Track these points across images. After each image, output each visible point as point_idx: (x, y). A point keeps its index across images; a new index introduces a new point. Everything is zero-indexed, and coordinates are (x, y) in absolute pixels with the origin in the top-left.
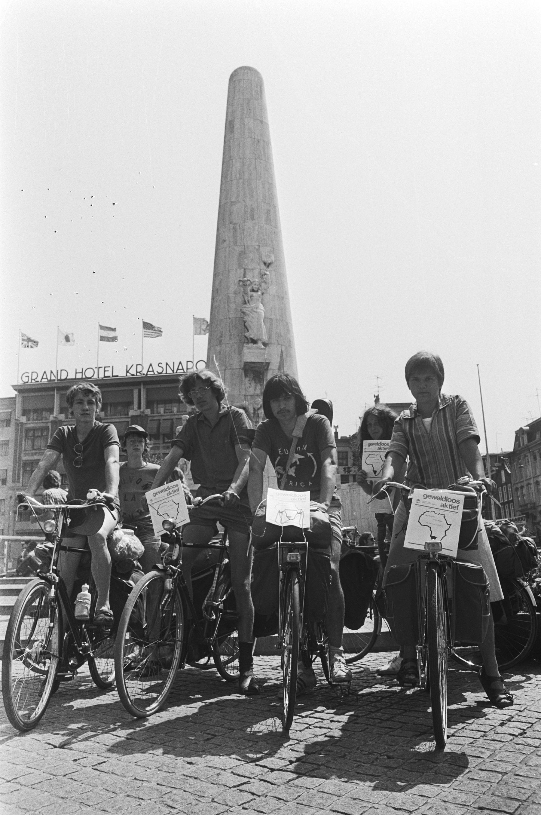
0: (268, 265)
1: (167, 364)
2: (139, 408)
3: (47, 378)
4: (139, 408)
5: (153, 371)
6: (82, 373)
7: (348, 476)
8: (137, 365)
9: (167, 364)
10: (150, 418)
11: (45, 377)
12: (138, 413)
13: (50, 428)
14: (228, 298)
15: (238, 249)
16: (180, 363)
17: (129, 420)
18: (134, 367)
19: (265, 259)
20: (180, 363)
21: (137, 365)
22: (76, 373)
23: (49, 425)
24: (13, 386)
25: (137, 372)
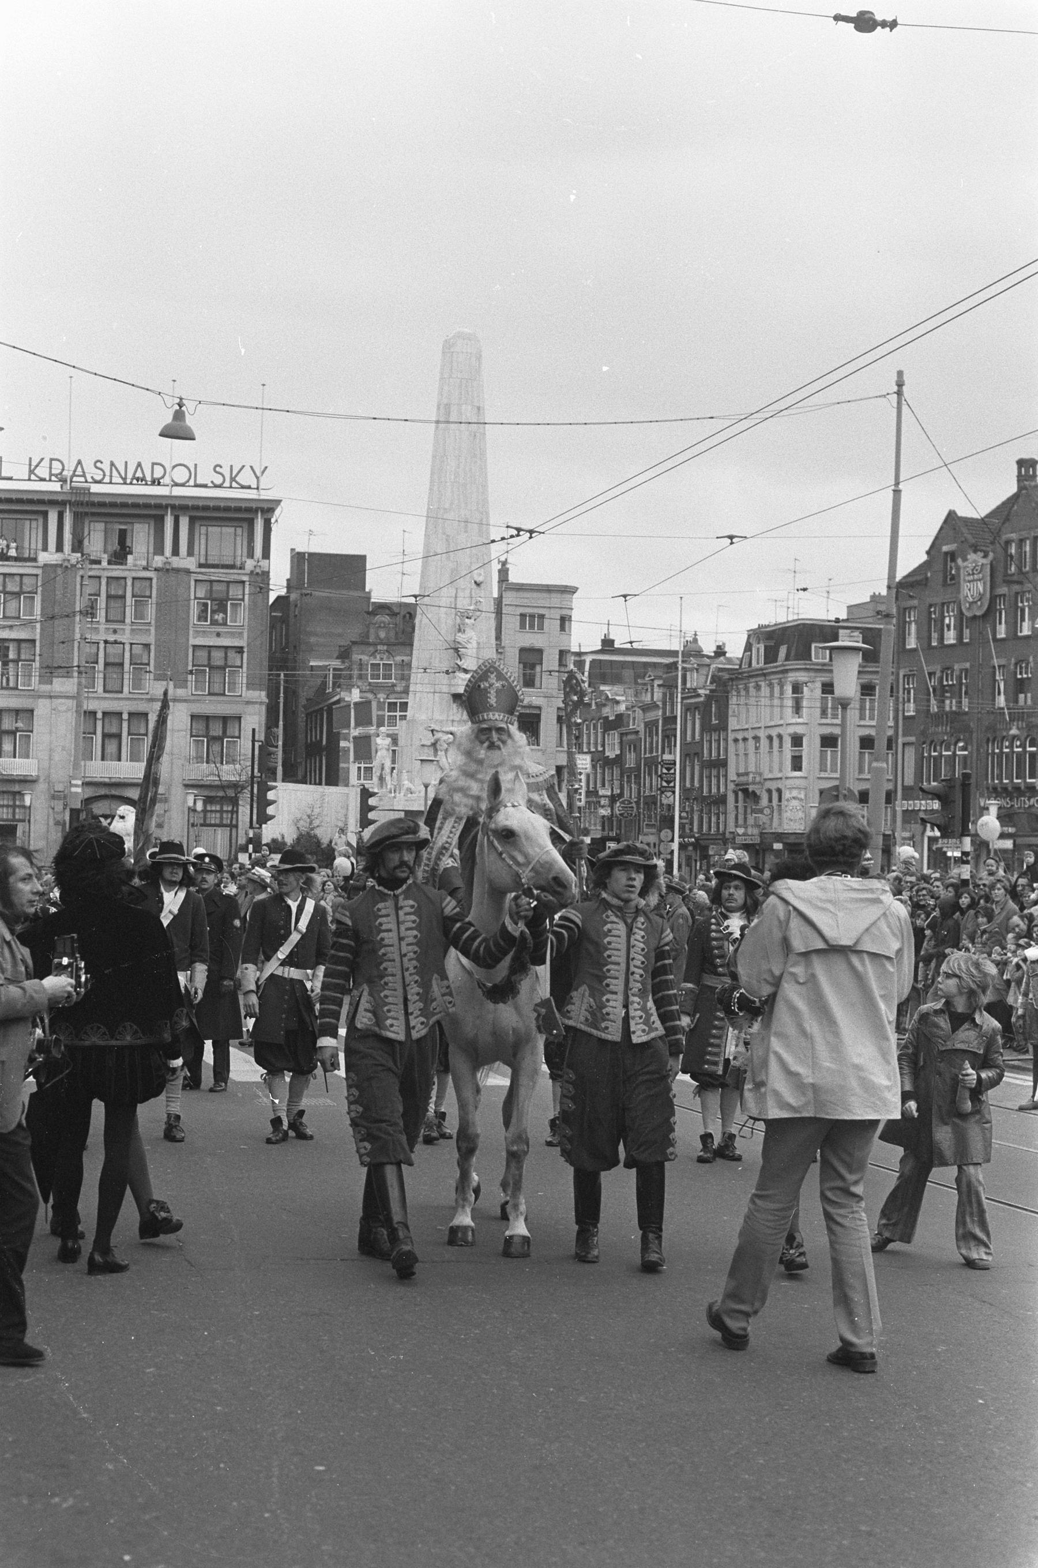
1: (112, 464)
2: (60, 548)
5: (84, 476)
8: (51, 460)
9: (112, 464)
16: (139, 465)
18: (46, 463)
20: (139, 465)
21: (51, 460)
25: (51, 475)
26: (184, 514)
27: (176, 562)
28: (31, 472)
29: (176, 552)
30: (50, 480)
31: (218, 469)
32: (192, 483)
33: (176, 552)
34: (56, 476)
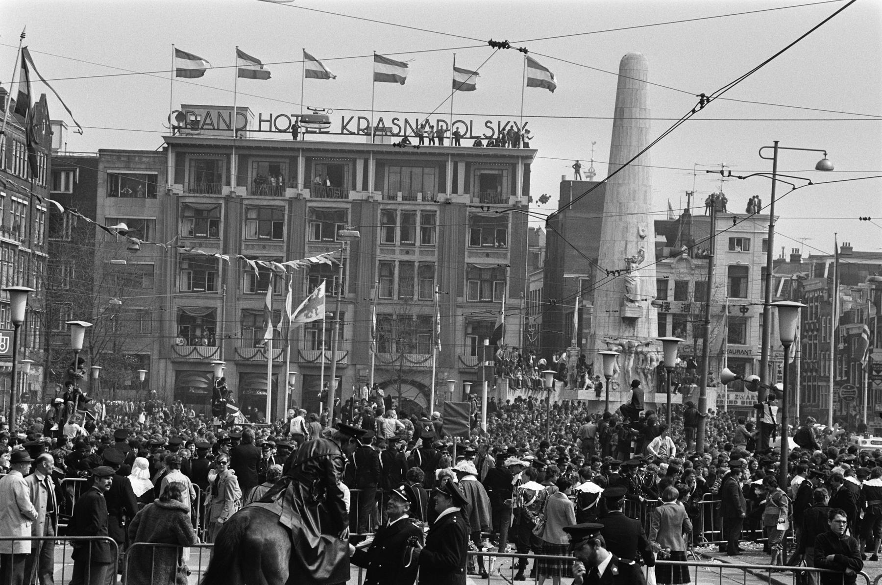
0: (642, 237)
1: (406, 121)
2: (365, 187)
3: (212, 124)
4: (365, 187)
6: (270, 121)
7: (666, 314)
8: (359, 118)
9: (406, 121)
10: (381, 207)
11: (208, 121)
12: (362, 196)
13: (223, 206)
14: (614, 262)
15: (622, 225)
17: (349, 206)
18: (355, 120)
19: (642, 234)
21: (359, 118)
22: (261, 121)
23: (222, 202)
24: (164, 137)
25: (359, 130)
26: (461, 161)
27: (455, 199)
28: (344, 127)
29: (455, 190)
30: (358, 134)
31: (489, 124)
32: (468, 135)
33: (455, 190)
34: (363, 130)
